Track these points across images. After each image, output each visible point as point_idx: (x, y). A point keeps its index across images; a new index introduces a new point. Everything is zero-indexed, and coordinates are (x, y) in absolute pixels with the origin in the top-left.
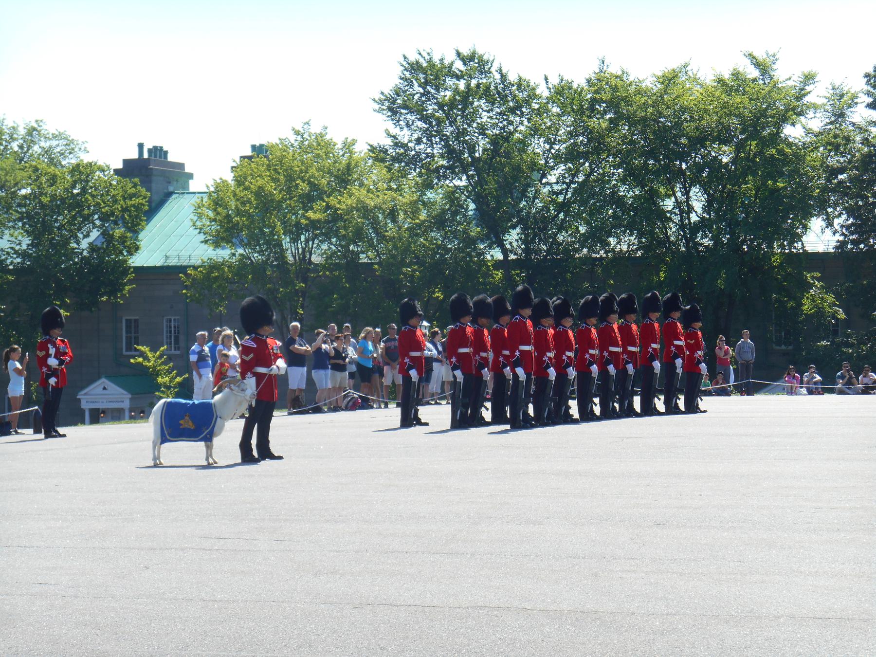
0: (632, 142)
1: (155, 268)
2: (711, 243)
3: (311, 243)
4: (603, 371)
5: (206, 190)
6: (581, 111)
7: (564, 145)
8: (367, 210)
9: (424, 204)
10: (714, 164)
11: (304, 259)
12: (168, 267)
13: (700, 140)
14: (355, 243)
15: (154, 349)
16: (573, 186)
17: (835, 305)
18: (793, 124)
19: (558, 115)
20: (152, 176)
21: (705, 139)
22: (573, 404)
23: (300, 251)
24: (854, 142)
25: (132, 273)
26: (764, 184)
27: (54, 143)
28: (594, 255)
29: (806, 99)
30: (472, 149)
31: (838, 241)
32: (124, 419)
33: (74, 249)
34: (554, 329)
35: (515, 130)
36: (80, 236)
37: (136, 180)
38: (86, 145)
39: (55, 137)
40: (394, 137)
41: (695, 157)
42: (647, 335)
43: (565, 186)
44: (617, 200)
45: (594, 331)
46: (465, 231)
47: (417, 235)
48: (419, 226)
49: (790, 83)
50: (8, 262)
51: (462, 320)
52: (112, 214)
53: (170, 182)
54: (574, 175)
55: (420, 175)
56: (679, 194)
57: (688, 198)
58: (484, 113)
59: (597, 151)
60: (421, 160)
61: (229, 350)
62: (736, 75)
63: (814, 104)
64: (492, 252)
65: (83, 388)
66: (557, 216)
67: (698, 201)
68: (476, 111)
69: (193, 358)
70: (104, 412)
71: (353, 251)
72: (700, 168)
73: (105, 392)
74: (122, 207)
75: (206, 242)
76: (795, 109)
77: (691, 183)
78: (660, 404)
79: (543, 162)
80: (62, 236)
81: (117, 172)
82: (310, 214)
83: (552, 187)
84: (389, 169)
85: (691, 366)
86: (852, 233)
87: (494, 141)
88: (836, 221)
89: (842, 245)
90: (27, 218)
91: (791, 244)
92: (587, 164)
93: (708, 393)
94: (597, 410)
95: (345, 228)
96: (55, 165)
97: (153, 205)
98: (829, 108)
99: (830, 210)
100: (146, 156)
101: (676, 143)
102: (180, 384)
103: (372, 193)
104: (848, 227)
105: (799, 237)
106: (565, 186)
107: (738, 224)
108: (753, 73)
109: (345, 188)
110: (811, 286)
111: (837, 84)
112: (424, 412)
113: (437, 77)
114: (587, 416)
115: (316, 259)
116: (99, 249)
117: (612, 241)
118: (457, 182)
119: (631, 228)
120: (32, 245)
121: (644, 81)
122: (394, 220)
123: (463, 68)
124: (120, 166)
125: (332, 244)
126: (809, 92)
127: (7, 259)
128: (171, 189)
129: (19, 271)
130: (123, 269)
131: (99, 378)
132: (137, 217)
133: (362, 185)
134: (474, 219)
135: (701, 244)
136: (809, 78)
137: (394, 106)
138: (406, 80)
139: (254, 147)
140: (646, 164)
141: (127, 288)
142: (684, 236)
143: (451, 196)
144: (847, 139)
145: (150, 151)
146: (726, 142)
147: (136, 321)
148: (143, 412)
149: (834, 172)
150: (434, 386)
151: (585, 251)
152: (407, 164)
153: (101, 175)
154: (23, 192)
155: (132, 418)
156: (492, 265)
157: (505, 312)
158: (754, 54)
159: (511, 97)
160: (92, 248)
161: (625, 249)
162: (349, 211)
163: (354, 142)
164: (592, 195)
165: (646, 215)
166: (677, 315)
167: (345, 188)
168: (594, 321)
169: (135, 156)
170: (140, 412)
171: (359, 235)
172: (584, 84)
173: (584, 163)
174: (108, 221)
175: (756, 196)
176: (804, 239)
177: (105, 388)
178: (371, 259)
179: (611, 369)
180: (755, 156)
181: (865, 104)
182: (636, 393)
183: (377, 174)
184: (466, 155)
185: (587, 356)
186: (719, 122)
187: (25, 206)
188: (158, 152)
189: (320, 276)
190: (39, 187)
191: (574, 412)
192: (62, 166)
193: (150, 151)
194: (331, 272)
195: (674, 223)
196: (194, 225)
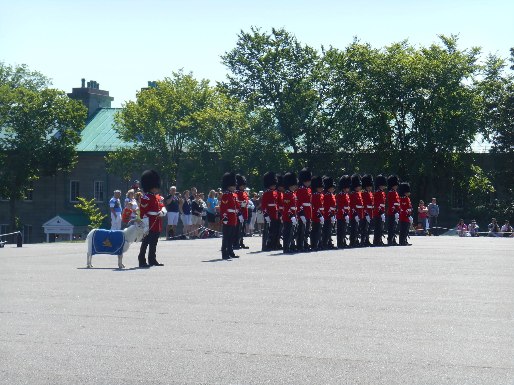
0: (371, 86)
1: (90, 152)
2: (417, 146)
3: (181, 140)
4: (352, 219)
5: (121, 107)
6: (342, 67)
7: (332, 87)
8: (215, 121)
9: (249, 119)
10: (419, 99)
11: (177, 150)
12: (98, 152)
13: (412, 85)
14: (208, 141)
15: (88, 200)
16: (336, 110)
18: (467, 77)
19: (328, 69)
20: (90, 98)
21: (415, 85)
22: (334, 238)
23: (175, 144)
24: (503, 89)
25: (76, 155)
26: (449, 113)
27: (33, 78)
28: (348, 152)
29: (476, 63)
30: (278, 87)
31: (492, 147)
32: (69, 240)
33: (42, 140)
34: (324, 194)
35: (303, 77)
36: (47, 132)
37: (81, 101)
38: (52, 80)
39: (33, 75)
40: (232, 79)
41: (409, 96)
42: (378, 199)
43: (331, 111)
44: (362, 120)
45: (347, 196)
46: (272, 135)
47: (244, 137)
48: (246, 131)
49: (465, 53)
50: (4, 147)
51: (271, 188)
52: (66, 120)
53: (99, 102)
54: (337, 105)
55: (246, 101)
56: (398, 117)
57: (404, 119)
58: (286, 67)
59: (351, 90)
60: (248, 93)
61: (132, 201)
62: (433, 48)
63: (478, 65)
64: (288, 148)
65: (46, 221)
66: (326, 128)
67: (409, 121)
68: (281, 65)
69: (112, 205)
70: (57, 235)
71: (206, 146)
72: (411, 102)
73: (59, 224)
74: (71, 116)
75: (120, 138)
76: (468, 68)
77: (406, 111)
78: (385, 239)
79: (319, 96)
80: (36, 132)
81: (69, 95)
82: (181, 123)
83: (324, 111)
84: (228, 97)
85: (404, 218)
86: (500, 142)
87: (291, 83)
89: (494, 149)
90: (15, 121)
91: (464, 147)
92: (345, 98)
93: (413, 234)
94: (348, 242)
95: (202, 132)
96: (34, 91)
97: (90, 115)
98: (487, 69)
99: (487, 129)
100: (86, 86)
101: (397, 87)
102: (103, 221)
103: (219, 111)
104: (497, 139)
105: (469, 144)
106: (331, 111)
107: (432, 135)
108: (444, 47)
109: (203, 108)
110: (474, 173)
111: (493, 54)
112: (247, 241)
113: (259, 44)
114: (342, 245)
115: (184, 149)
116: (58, 140)
117: (359, 144)
118: (268, 107)
119: (370, 136)
120: (18, 137)
121: (379, 50)
122: (231, 128)
123: (275, 40)
124: (71, 92)
125: (194, 141)
126: (476, 59)
127: (3, 145)
128: (100, 106)
129: (9, 152)
130: (71, 152)
131: (55, 216)
132: (80, 122)
133: (212, 106)
134: (278, 128)
135: (411, 147)
136: (476, 51)
137: (233, 60)
138: (240, 45)
139: (149, 83)
140: (379, 99)
141: (73, 163)
142: (401, 142)
143: (265, 114)
144: (499, 87)
145: (88, 83)
146: (427, 88)
147: (78, 183)
148: (80, 236)
149: (490, 106)
150: (252, 226)
151: (342, 149)
152: (239, 95)
153: (60, 97)
154: (14, 105)
155: (74, 239)
156: (288, 156)
157: (294, 183)
158: (445, 36)
159: (302, 57)
160: (53, 139)
161: (366, 148)
162: (205, 121)
163: (208, 81)
164: (348, 116)
165: (380, 128)
166: (396, 188)
167: (203, 108)
168: (347, 190)
169: (80, 86)
170: (79, 236)
171: (209, 136)
172: (344, 50)
173: (343, 98)
174: (63, 124)
175: (444, 120)
176: (472, 145)
177: (58, 222)
178: (216, 150)
179: (357, 218)
180: (444, 95)
181: (509, 66)
182: (371, 233)
183: (220, 100)
184: (274, 91)
185: (343, 210)
186: (423, 76)
187: (14, 113)
188: (93, 84)
189: (186, 160)
190: (23, 103)
191: (335, 243)
192: (38, 92)
193: (88, 83)
194: (193, 157)
195: (395, 134)
196: (113, 127)
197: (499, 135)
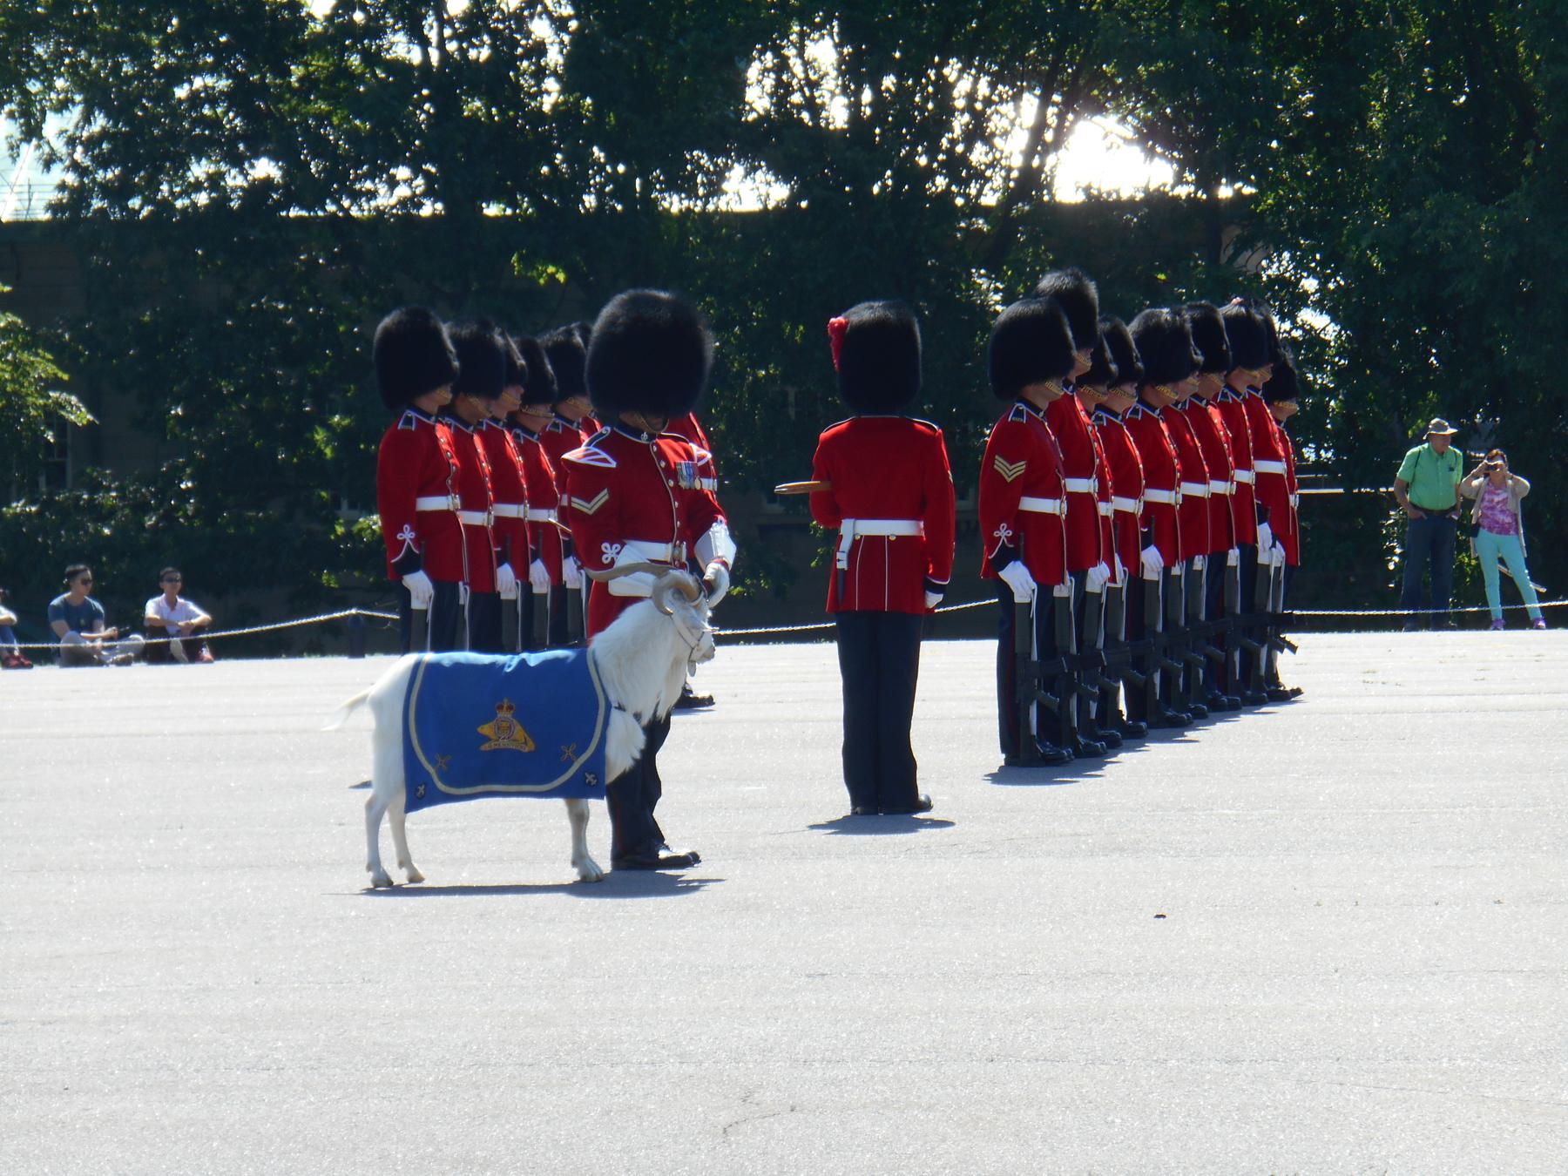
31: (62, 187)
86: (103, 162)
88: (54, 125)
89: (79, 196)
99: (34, 86)
104: (91, 144)
197: (100, 122)
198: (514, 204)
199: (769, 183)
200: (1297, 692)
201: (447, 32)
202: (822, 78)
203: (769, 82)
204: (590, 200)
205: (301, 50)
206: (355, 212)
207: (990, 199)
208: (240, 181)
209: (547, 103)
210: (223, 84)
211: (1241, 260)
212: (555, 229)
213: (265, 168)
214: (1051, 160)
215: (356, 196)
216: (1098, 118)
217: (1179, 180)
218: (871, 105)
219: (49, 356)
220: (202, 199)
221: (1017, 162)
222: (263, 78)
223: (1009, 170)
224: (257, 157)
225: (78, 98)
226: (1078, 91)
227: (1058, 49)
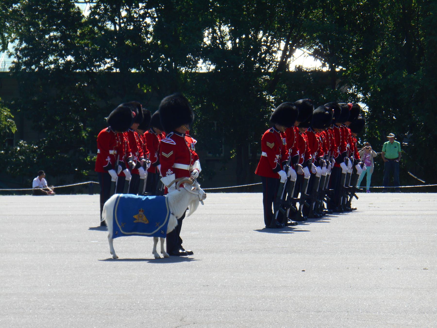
17: (10, 118)
31: (13, 62)
89: (17, 65)
104: (22, 51)
198: (138, 69)
199: (209, 64)
200: (356, 209)
201: (121, 21)
202: (225, 36)
203: (210, 37)
204: (160, 69)
205: (82, 26)
206: (94, 71)
207: (271, 70)
208: (63, 61)
209: (149, 41)
210: (58, 34)
211: (341, 88)
212: (149, 76)
213: (69, 58)
214: (289, 60)
215: (95, 66)
216: (302, 48)
217: (324, 65)
218: (238, 43)
219: (9, 110)
220: (52, 66)
221: (279, 59)
222: (70, 33)
223: (277, 62)
224: (68, 55)
225: (18, 38)
226: (296, 42)
227: (291, 29)
